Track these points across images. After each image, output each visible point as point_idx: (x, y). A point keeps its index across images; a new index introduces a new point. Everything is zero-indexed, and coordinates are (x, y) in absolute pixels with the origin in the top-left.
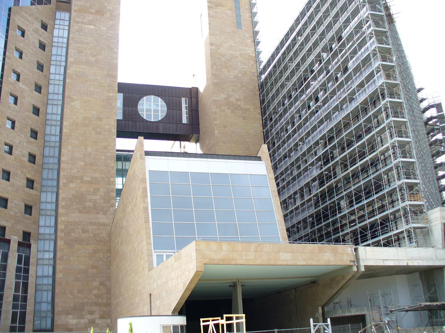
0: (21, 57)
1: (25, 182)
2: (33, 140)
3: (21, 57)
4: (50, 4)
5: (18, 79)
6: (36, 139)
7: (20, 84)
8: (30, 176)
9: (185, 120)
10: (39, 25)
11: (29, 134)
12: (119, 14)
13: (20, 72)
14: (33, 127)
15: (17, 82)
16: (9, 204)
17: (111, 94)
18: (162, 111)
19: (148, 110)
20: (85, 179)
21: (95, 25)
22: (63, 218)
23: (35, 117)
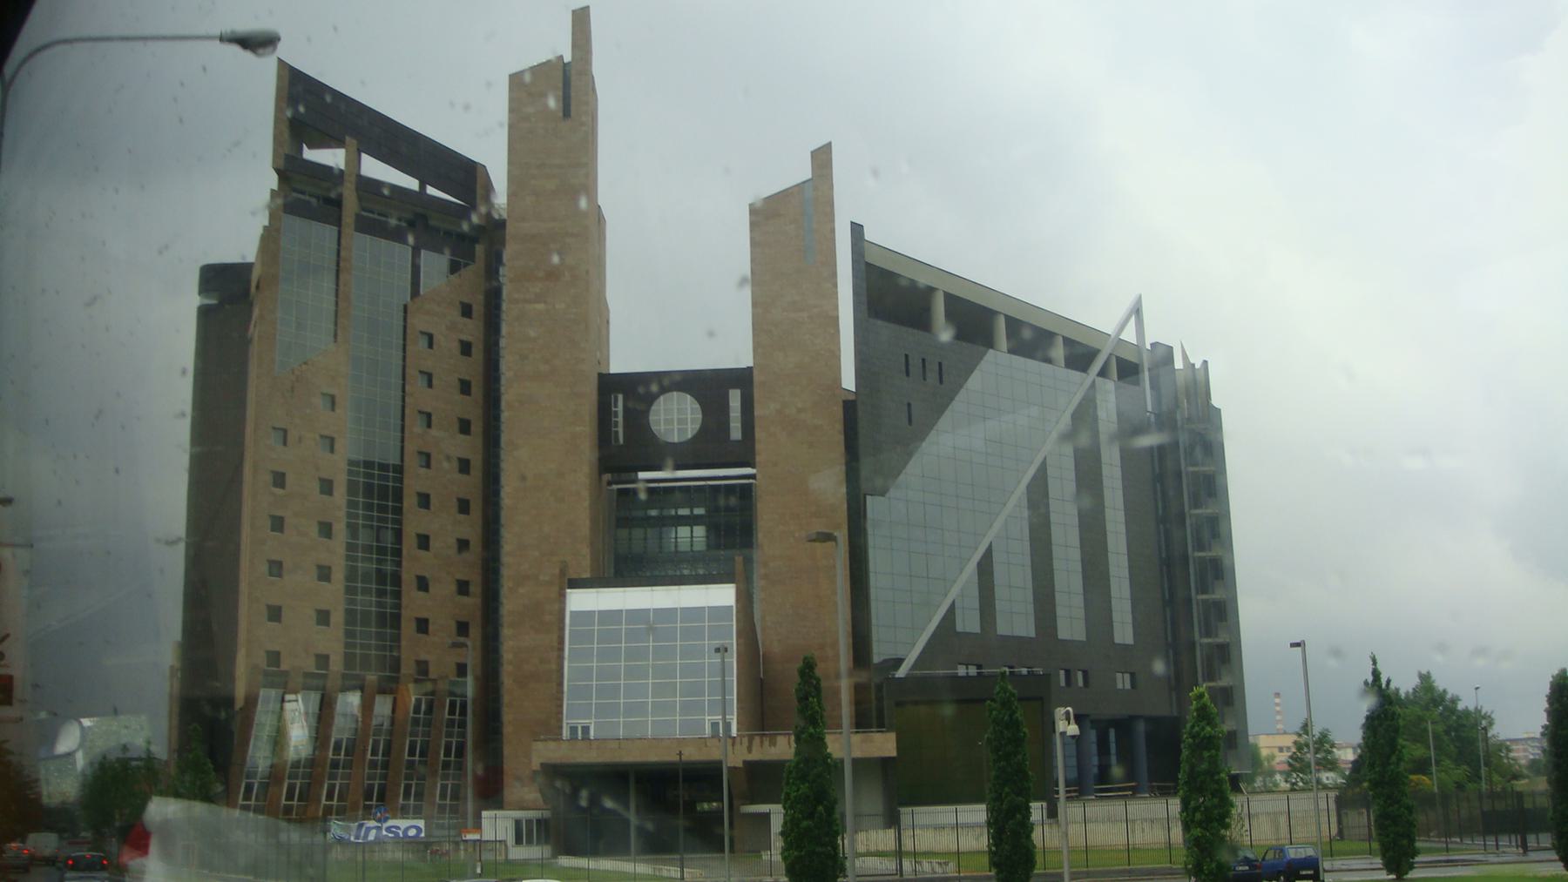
0: (430, 385)
1: (454, 588)
2: (462, 517)
3: (430, 385)
4: (474, 261)
5: (429, 425)
6: (468, 513)
7: (434, 432)
8: (459, 576)
9: (736, 433)
10: (455, 314)
11: (453, 505)
12: (587, 272)
13: (429, 410)
14: (461, 496)
15: (428, 430)
16: (431, 628)
17: (578, 429)
18: (693, 421)
19: (668, 422)
20: (541, 578)
21: (545, 302)
22: (511, 643)
23: (464, 477)
